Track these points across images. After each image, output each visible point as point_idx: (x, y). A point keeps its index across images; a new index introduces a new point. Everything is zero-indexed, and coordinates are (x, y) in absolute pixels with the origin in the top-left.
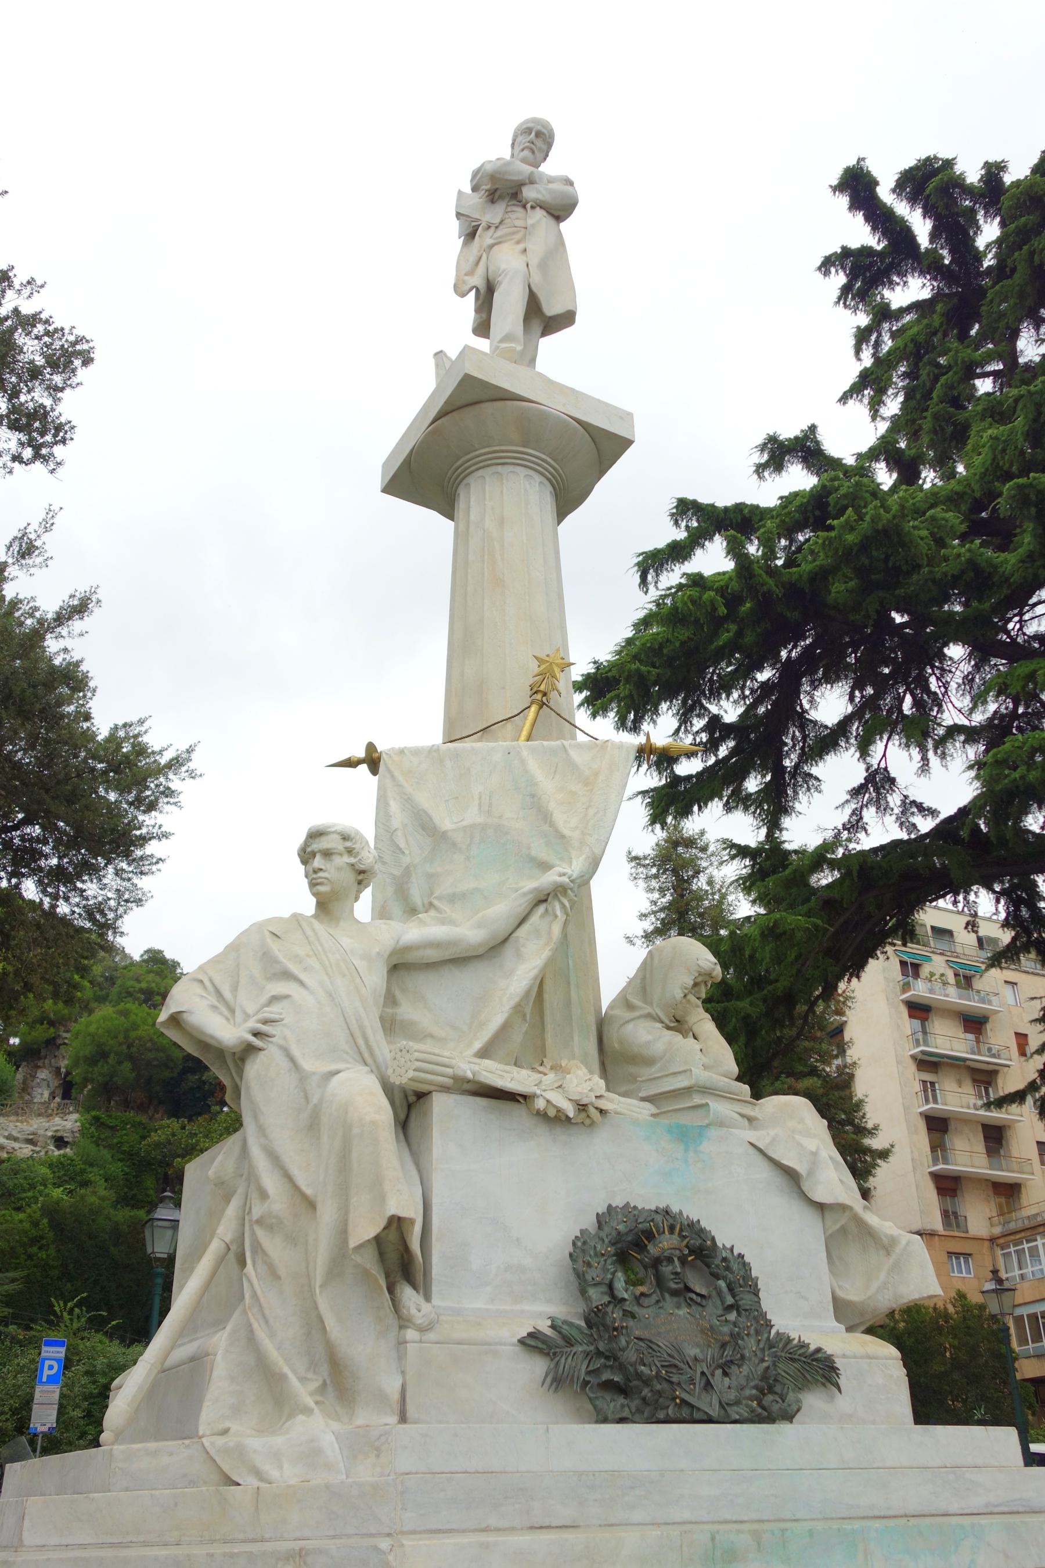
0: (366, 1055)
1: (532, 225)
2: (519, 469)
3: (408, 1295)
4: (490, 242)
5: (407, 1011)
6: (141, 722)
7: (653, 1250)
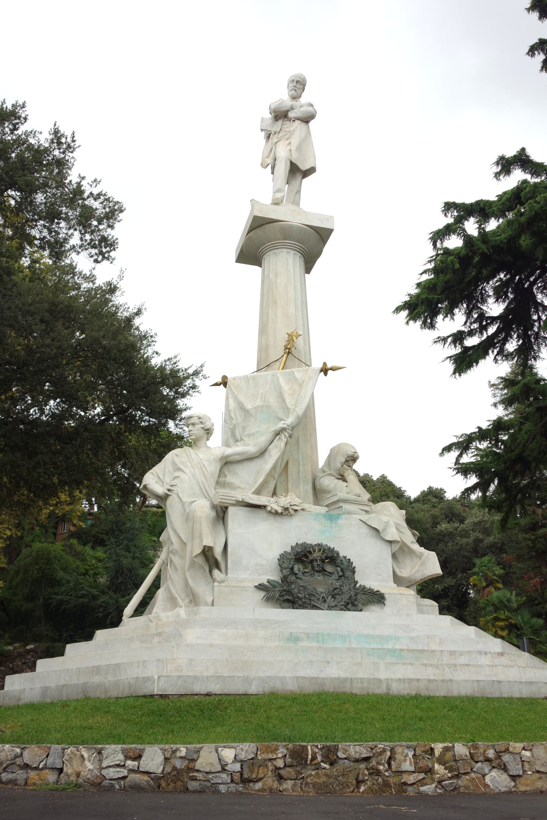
0: (206, 495)
1: (293, 130)
2: (284, 250)
3: (216, 572)
4: (275, 140)
5: (230, 478)
6: (175, 357)
7: (311, 558)
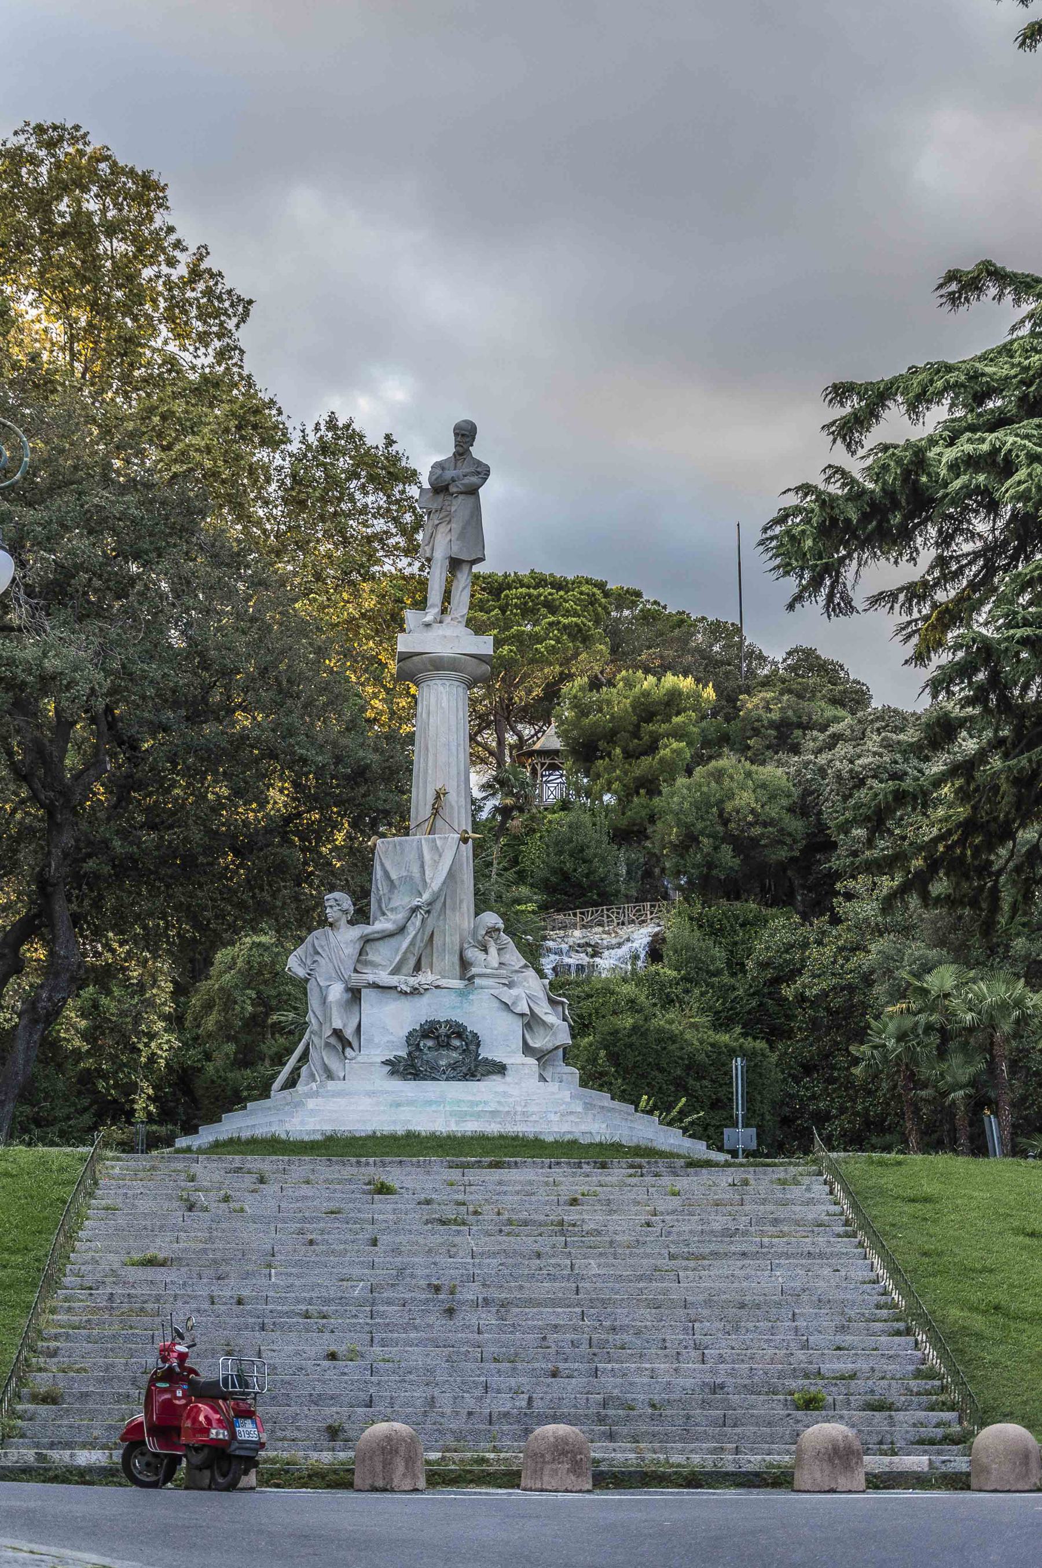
3: (348, 1050)
5: (371, 957)
